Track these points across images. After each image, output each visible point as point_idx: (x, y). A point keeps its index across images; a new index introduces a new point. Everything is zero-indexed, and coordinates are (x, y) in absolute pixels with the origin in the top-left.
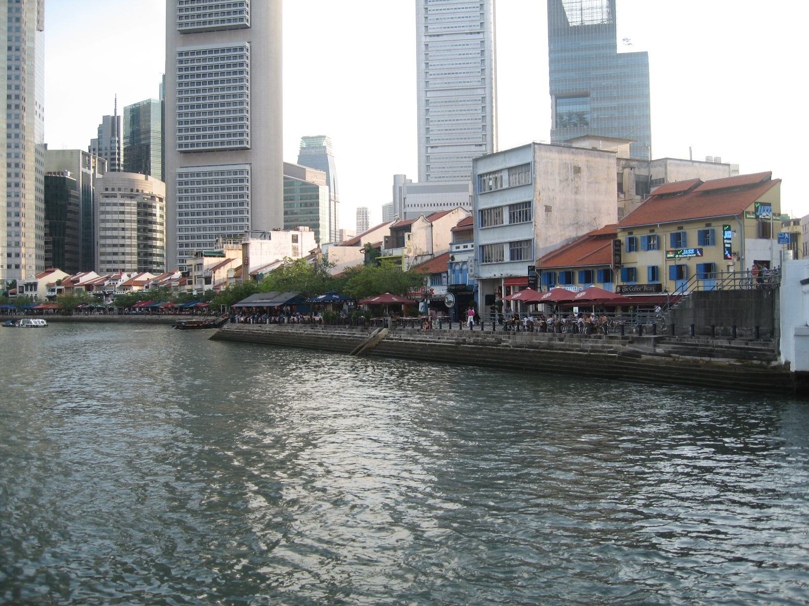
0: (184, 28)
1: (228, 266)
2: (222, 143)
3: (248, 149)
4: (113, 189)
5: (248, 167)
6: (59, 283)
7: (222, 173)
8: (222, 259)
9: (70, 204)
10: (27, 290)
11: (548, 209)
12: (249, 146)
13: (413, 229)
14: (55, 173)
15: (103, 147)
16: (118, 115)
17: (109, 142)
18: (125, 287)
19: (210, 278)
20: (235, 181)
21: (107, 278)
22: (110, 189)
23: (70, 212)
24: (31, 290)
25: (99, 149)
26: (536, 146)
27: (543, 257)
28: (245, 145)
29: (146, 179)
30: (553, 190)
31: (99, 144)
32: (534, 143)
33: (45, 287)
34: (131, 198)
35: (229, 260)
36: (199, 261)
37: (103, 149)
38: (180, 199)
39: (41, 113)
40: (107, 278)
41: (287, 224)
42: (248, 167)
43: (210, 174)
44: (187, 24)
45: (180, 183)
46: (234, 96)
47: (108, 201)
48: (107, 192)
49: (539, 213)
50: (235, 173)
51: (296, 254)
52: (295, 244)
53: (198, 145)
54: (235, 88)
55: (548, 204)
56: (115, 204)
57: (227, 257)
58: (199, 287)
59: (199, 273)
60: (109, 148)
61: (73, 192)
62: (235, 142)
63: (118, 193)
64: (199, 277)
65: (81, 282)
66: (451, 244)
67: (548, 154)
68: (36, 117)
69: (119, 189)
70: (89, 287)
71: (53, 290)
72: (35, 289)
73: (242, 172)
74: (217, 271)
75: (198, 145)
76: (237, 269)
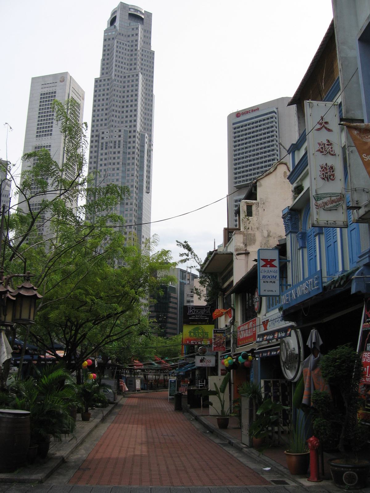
0: (238, 184)
9: (170, 302)
23: (172, 308)
44: (240, 182)
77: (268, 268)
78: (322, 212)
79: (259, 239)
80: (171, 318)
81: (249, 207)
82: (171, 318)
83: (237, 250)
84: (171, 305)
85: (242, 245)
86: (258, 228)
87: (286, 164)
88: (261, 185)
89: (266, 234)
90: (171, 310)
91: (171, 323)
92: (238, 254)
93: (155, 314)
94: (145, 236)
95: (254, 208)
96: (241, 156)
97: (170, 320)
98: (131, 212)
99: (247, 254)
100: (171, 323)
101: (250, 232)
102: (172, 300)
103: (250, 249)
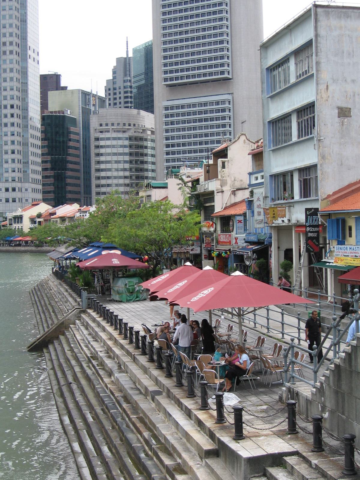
2: (205, 75)
3: (230, 79)
4: (107, 125)
5: (229, 97)
6: (39, 216)
7: (205, 104)
9: (70, 140)
10: (15, 223)
11: (344, 113)
12: (230, 77)
13: (230, 153)
14: (55, 112)
15: (117, 86)
16: (129, 56)
17: (122, 82)
20: (218, 111)
22: (104, 125)
24: (18, 223)
25: (115, 89)
26: (319, 10)
27: (335, 193)
28: (226, 75)
29: (139, 114)
30: (353, 81)
31: (114, 83)
32: (316, 6)
33: (28, 220)
34: (124, 132)
36: (148, 193)
37: (117, 88)
39: (36, 57)
42: (229, 97)
43: (194, 105)
45: (167, 116)
46: (215, 28)
48: (101, 128)
49: (326, 118)
50: (217, 103)
53: (182, 78)
54: (215, 20)
55: (344, 105)
56: (108, 139)
60: (122, 87)
61: (72, 129)
62: (216, 73)
63: (110, 127)
66: (250, 174)
67: (343, 23)
68: (30, 61)
69: (113, 124)
70: (63, 219)
71: (35, 222)
72: (21, 222)
73: (223, 102)
75: (182, 78)
77: (240, 224)
78: (257, 225)
79: (229, 182)
80: (71, 163)
81: (223, 163)
82: (71, 163)
83: (217, 190)
84: (71, 144)
85: (220, 187)
86: (228, 176)
87: (245, 135)
88: (230, 149)
89: (233, 179)
90: (71, 151)
91: (72, 170)
92: (218, 192)
93: (49, 158)
94: (32, 47)
95: (226, 164)
96: (202, 64)
97: (70, 166)
98: (11, 12)
99: (222, 192)
100: (72, 170)
101: (224, 178)
102: (72, 136)
103: (224, 189)
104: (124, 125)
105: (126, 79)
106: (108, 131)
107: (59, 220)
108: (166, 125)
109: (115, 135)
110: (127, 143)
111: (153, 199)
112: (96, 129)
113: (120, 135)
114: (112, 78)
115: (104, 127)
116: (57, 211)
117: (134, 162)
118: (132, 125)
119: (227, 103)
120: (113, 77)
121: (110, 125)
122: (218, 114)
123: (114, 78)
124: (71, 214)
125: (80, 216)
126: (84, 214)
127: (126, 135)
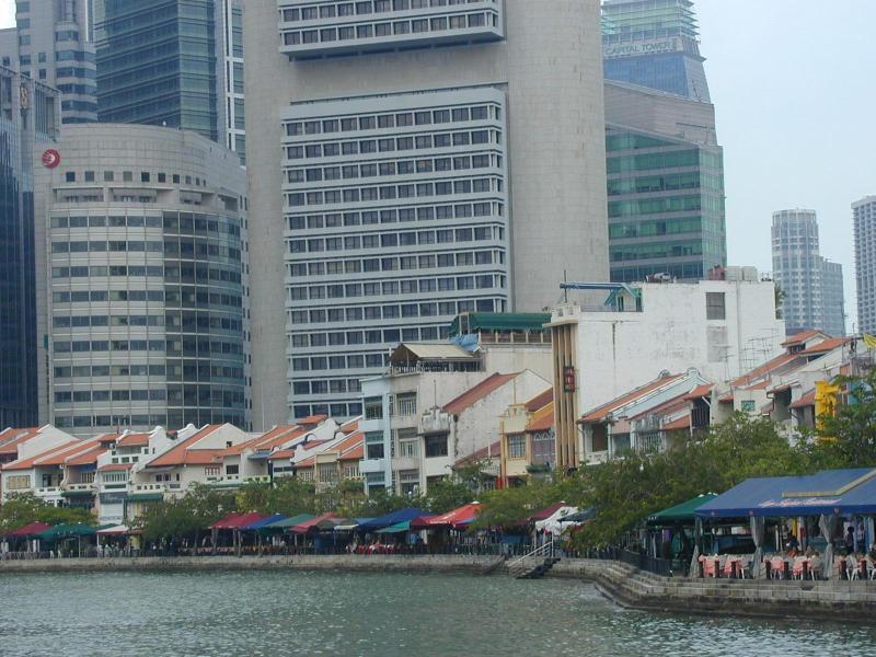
1: (503, 397)
8: (476, 378)
12: (500, 33)
15: (33, 51)
17: (52, 37)
18: (161, 471)
19: (444, 434)
21: (105, 444)
28: (486, 28)
34: (145, 199)
35: (496, 379)
36: (404, 386)
37: (35, 58)
38: (296, 199)
40: (105, 444)
41: (619, 264)
45: (293, 152)
47: (76, 210)
48: (72, 185)
51: (720, 354)
52: (717, 323)
53: (344, 32)
57: (490, 372)
58: (406, 463)
59: (408, 421)
60: (50, 56)
63: (100, 182)
64: (408, 433)
65: (21, 457)
74: (465, 415)
76: (532, 406)
104: (145, 177)
105: (62, 28)
106: (94, 198)
107: (33, 474)
108: (290, 181)
109: (118, 210)
110: (156, 234)
111: (424, 401)
112: (55, 191)
113: (136, 210)
114: (14, 24)
115: (81, 183)
116: (19, 445)
117: (179, 297)
118: (169, 179)
119: (491, 113)
120: (18, 21)
121: (99, 177)
122: (461, 148)
123: (22, 23)
124: (49, 456)
125: (115, 460)
126: (131, 456)
127: (154, 210)
